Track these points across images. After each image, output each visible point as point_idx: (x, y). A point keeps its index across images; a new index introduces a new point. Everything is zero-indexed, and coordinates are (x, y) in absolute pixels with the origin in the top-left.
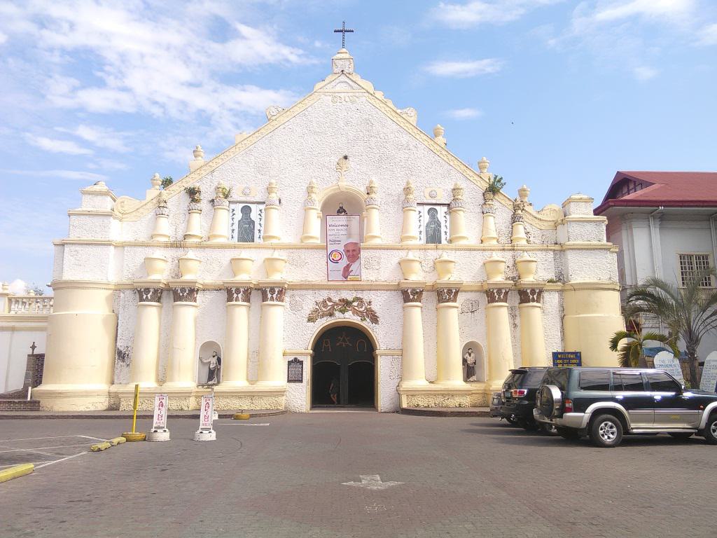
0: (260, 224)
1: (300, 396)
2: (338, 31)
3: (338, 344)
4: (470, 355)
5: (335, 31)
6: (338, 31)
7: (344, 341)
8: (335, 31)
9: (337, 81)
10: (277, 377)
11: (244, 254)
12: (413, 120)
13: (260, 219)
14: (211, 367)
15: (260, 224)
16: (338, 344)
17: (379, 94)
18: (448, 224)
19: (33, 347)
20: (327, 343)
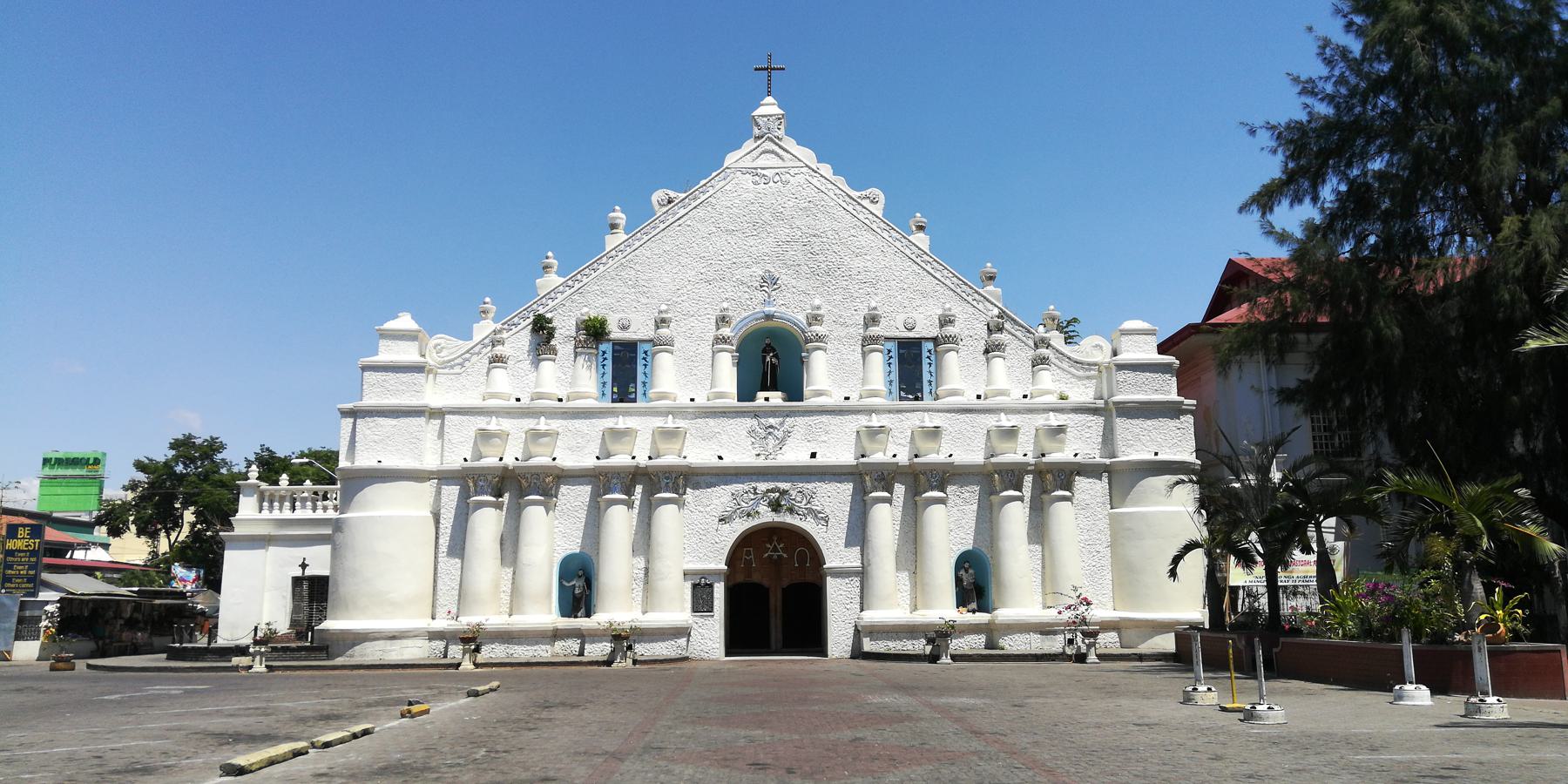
0: (645, 373)
1: (709, 636)
2: (759, 69)
3: (785, 555)
4: (966, 571)
5: (756, 69)
6: (759, 69)
7: (775, 549)
8: (756, 69)
9: (760, 150)
10: (675, 610)
11: (622, 423)
12: (878, 209)
13: (645, 365)
14: (577, 591)
15: (645, 373)
16: (785, 555)
17: (826, 169)
18: (933, 369)
19: (304, 566)
20: (748, 553)
